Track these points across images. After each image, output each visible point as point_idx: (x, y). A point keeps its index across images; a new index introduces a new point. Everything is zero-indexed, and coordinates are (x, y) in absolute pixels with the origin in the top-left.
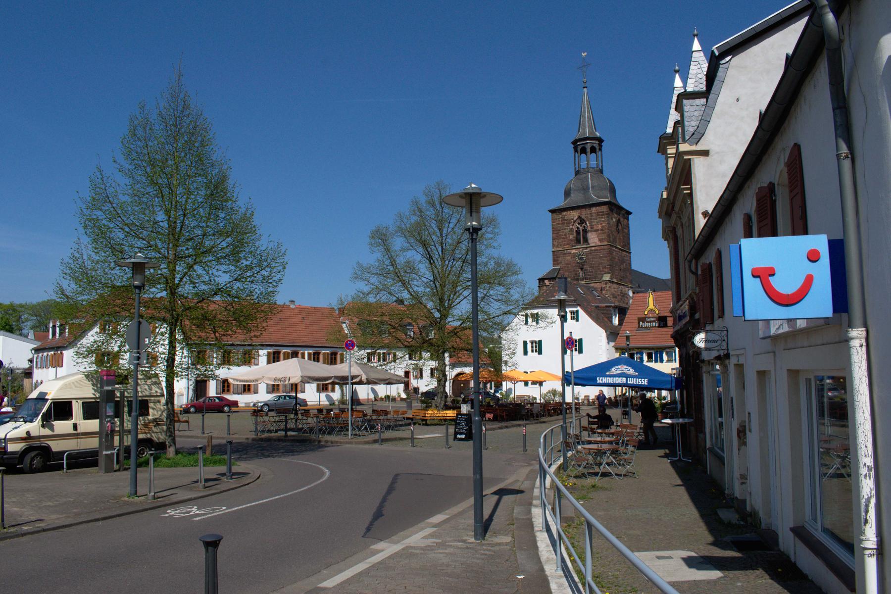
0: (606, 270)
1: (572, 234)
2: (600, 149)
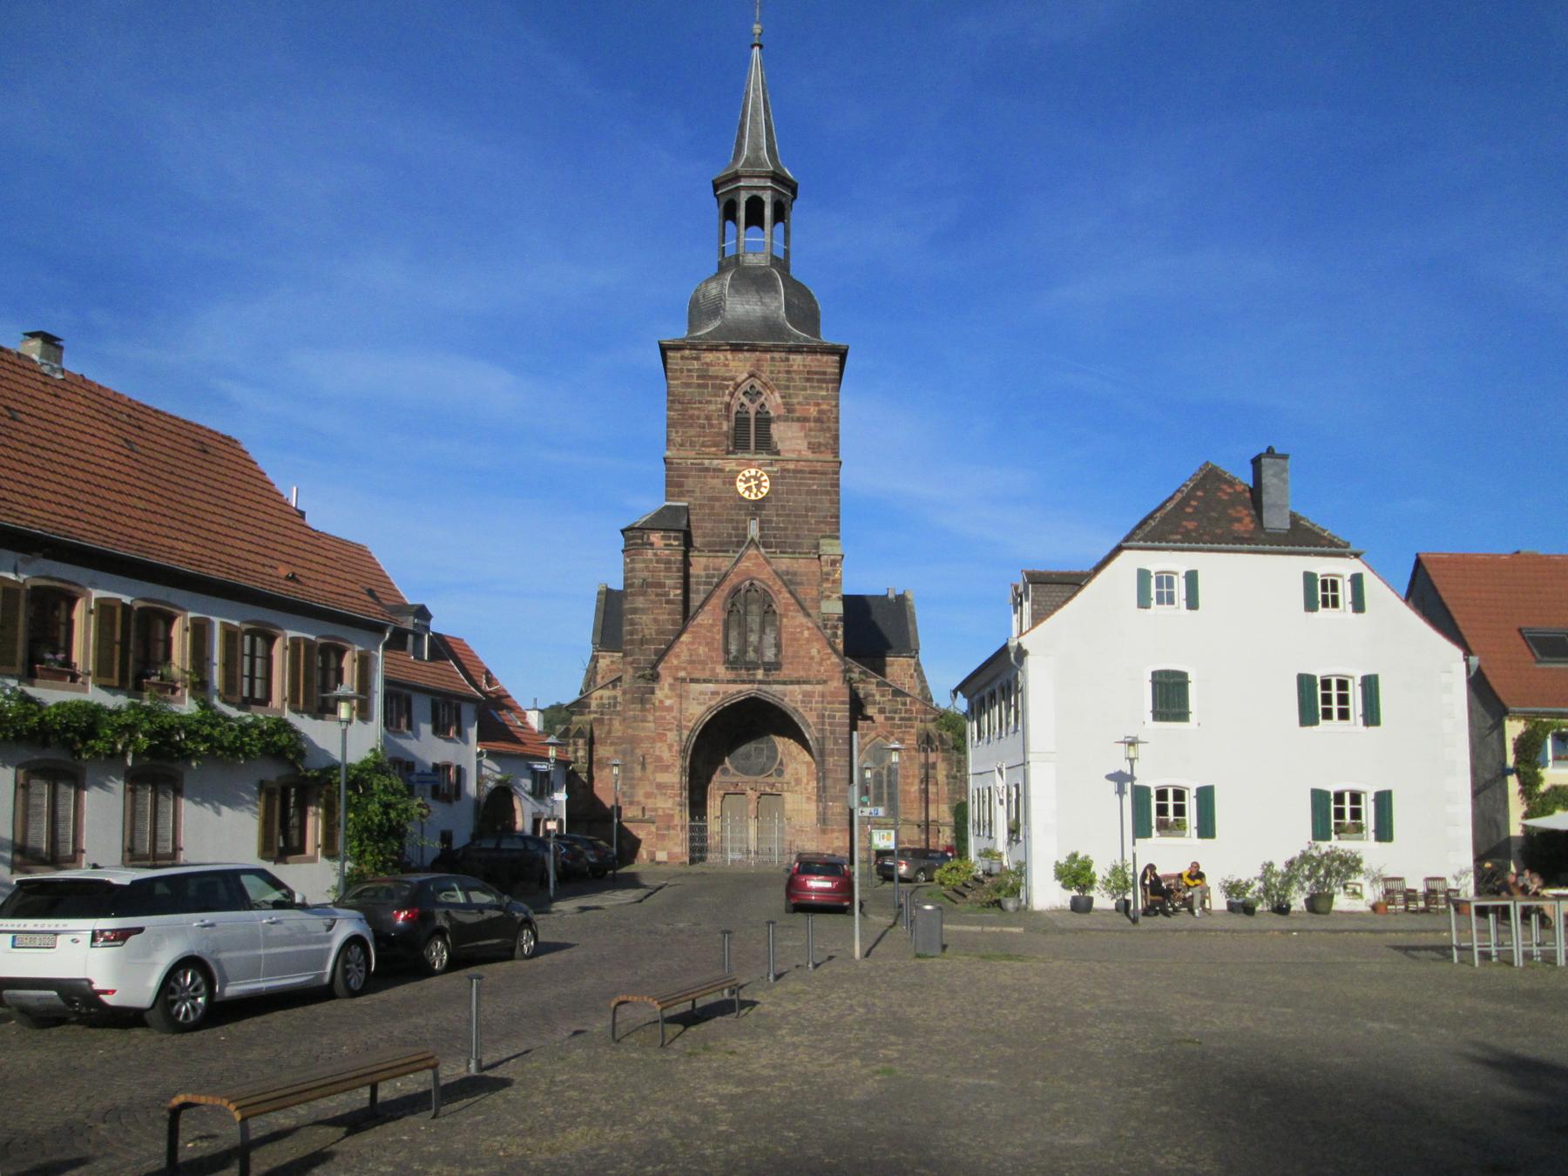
1: (728, 418)
2: (780, 214)
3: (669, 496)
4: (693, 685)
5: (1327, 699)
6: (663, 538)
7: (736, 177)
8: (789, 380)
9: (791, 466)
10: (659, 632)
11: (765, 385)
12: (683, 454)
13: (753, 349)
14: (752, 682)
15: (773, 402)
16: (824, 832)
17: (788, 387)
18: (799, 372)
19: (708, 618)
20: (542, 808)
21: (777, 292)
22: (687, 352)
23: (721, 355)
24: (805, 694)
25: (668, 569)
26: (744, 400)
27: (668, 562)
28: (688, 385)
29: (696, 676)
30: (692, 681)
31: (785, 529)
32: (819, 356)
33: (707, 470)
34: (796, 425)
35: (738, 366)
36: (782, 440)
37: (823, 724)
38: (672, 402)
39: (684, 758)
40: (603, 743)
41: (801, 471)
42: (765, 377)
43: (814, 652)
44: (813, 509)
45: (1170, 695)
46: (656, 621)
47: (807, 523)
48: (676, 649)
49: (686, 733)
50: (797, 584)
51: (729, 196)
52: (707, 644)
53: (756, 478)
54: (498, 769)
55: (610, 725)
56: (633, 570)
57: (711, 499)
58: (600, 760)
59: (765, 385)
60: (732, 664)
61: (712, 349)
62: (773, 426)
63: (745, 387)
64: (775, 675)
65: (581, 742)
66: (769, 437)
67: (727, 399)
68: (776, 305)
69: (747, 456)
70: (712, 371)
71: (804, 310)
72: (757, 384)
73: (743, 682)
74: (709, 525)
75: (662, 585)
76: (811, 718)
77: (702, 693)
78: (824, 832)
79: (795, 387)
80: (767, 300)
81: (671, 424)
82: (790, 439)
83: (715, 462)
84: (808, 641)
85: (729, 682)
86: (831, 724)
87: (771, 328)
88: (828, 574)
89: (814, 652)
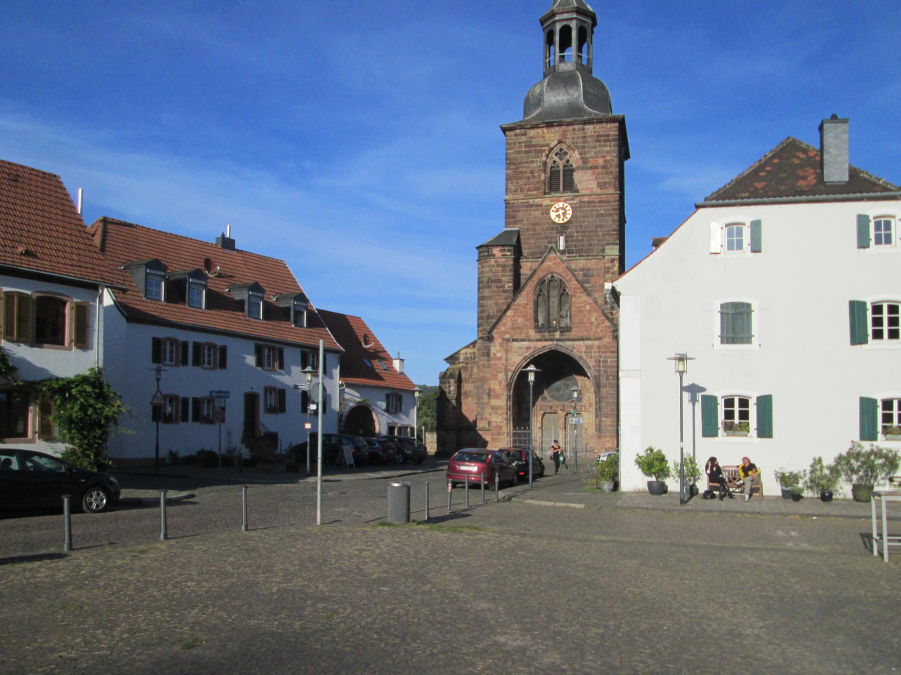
0: (611, 240)
3: (507, 224)
4: (515, 344)
5: (877, 322)
6: (501, 251)
7: (553, 14)
8: (584, 142)
9: (586, 199)
10: (498, 312)
11: (569, 147)
12: (516, 197)
13: (560, 124)
14: (552, 340)
15: (575, 157)
16: (599, 437)
17: (584, 147)
18: (592, 136)
19: (525, 298)
20: (396, 420)
21: (578, 86)
22: (518, 131)
23: (540, 131)
24: (587, 347)
25: (504, 271)
26: (556, 158)
27: (504, 266)
28: (519, 152)
29: (516, 337)
30: (514, 340)
31: (583, 240)
32: (604, 125)
33: (532, 206)
34: (589, 172)
35: (551, 136)
36: (580, 182)
37: (599, 366)
38: (510, 164)
39: (509, 390)
40: (467, 381)
41: (594, 202)
42: (568, 142)
43: (593, 319)
44: (601, 226)
45: (736, 323)
46: (497, 304)
47: (597, 236)
48: (504, 321)
49: (510, 374)
50: (590, 276)
51: (549, 28)
52: (523, 316)
53: (562, 208)
54: (358, 395)
55: (472, 370)
56: (482, 272)
57: (534, 224)
58: (465, 393)
59: (569, 147)
60: (538, 328)
61: (533, 127)
62: (575, 174)
63: (556, 150)
64: (567, 335)
65: (452, 381)
66: (572, 181)
67: (544, 159)
68: (577, 94)
69: (557, 195)
70: (534, 142)
71: (598, 96)
72: (564, 147)
73: (546, 340)
74: (533, 242)
75: (501, 281)
76: (591, 363)
77: (520, 348)
78: (599, 437)
79: (589, 147)
80: (571, 92)
81: (508, 178)
82: (585, 181)
83: (537, 200)
84: (589, 312)
85: (537, 340)
86: (604, 367)
87: (573, 109)
88: (609, 268)
89: (593, 319)
